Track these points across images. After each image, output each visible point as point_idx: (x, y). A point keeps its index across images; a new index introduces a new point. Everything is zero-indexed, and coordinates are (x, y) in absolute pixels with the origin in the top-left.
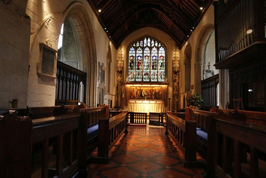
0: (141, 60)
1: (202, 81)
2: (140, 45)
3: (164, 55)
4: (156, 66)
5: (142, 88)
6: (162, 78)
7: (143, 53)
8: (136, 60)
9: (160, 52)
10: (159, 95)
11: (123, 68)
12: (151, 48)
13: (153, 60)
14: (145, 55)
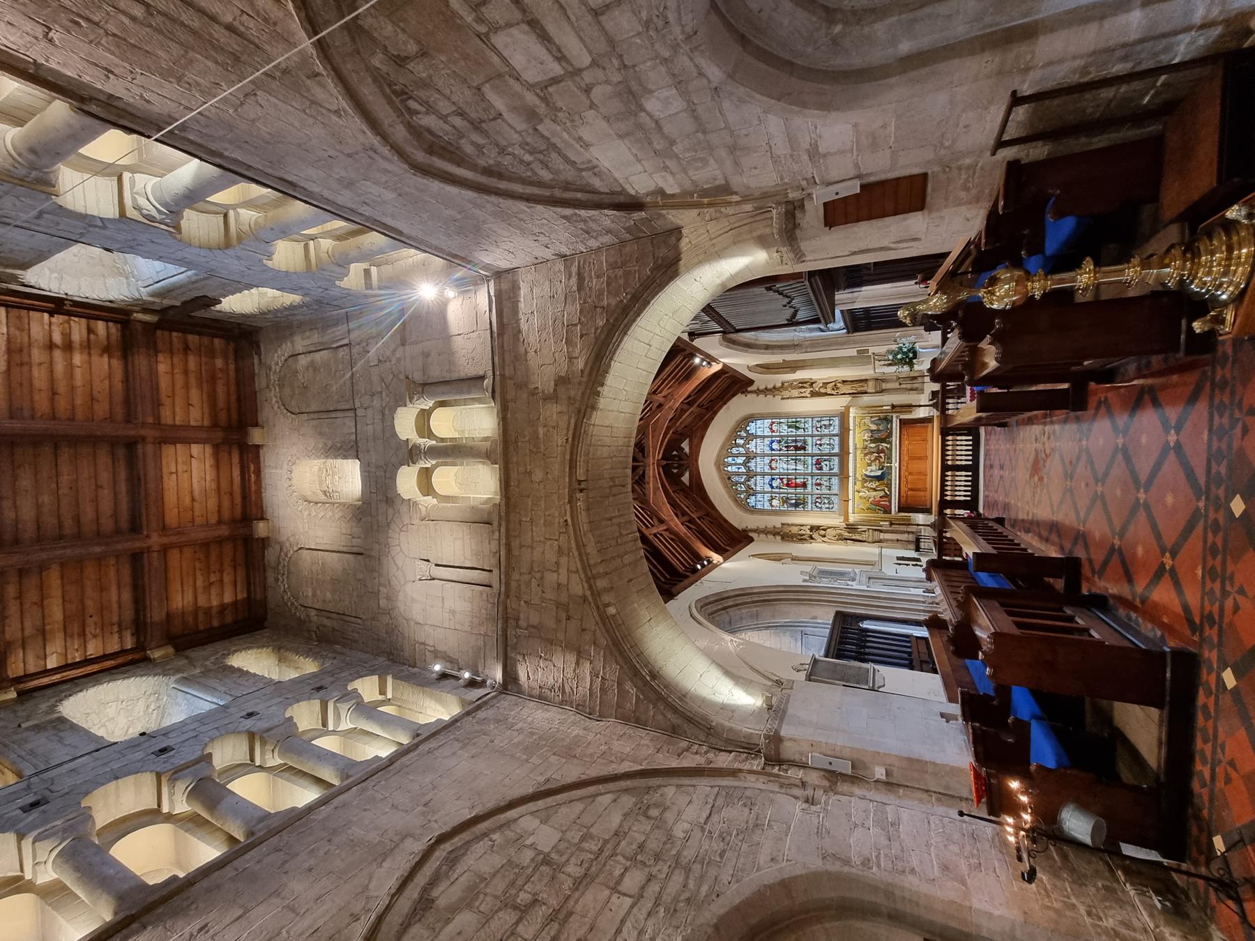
0: (781, 479)
1: (848, 332)
3: (767, 422)
4: (796, 441)
5: (858, 476)
6: (830, 425)
7: (763, 475)
9: (759, 433)
10: (878, 430)
12: (749, 457)
13: (780, 450)
14: (767, 469)
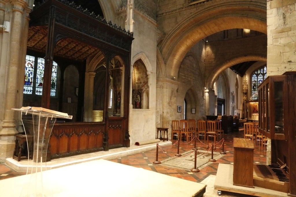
2: (260, 72)
8: (257, 83)
11: (247, 90)
